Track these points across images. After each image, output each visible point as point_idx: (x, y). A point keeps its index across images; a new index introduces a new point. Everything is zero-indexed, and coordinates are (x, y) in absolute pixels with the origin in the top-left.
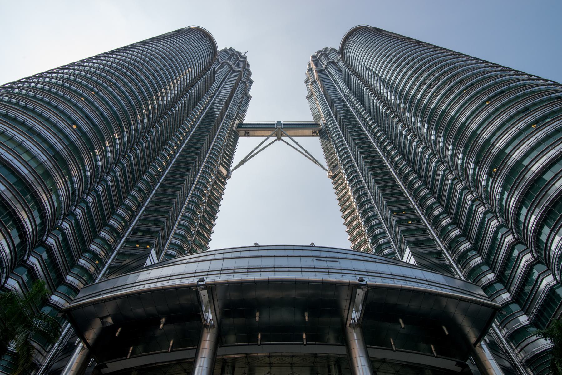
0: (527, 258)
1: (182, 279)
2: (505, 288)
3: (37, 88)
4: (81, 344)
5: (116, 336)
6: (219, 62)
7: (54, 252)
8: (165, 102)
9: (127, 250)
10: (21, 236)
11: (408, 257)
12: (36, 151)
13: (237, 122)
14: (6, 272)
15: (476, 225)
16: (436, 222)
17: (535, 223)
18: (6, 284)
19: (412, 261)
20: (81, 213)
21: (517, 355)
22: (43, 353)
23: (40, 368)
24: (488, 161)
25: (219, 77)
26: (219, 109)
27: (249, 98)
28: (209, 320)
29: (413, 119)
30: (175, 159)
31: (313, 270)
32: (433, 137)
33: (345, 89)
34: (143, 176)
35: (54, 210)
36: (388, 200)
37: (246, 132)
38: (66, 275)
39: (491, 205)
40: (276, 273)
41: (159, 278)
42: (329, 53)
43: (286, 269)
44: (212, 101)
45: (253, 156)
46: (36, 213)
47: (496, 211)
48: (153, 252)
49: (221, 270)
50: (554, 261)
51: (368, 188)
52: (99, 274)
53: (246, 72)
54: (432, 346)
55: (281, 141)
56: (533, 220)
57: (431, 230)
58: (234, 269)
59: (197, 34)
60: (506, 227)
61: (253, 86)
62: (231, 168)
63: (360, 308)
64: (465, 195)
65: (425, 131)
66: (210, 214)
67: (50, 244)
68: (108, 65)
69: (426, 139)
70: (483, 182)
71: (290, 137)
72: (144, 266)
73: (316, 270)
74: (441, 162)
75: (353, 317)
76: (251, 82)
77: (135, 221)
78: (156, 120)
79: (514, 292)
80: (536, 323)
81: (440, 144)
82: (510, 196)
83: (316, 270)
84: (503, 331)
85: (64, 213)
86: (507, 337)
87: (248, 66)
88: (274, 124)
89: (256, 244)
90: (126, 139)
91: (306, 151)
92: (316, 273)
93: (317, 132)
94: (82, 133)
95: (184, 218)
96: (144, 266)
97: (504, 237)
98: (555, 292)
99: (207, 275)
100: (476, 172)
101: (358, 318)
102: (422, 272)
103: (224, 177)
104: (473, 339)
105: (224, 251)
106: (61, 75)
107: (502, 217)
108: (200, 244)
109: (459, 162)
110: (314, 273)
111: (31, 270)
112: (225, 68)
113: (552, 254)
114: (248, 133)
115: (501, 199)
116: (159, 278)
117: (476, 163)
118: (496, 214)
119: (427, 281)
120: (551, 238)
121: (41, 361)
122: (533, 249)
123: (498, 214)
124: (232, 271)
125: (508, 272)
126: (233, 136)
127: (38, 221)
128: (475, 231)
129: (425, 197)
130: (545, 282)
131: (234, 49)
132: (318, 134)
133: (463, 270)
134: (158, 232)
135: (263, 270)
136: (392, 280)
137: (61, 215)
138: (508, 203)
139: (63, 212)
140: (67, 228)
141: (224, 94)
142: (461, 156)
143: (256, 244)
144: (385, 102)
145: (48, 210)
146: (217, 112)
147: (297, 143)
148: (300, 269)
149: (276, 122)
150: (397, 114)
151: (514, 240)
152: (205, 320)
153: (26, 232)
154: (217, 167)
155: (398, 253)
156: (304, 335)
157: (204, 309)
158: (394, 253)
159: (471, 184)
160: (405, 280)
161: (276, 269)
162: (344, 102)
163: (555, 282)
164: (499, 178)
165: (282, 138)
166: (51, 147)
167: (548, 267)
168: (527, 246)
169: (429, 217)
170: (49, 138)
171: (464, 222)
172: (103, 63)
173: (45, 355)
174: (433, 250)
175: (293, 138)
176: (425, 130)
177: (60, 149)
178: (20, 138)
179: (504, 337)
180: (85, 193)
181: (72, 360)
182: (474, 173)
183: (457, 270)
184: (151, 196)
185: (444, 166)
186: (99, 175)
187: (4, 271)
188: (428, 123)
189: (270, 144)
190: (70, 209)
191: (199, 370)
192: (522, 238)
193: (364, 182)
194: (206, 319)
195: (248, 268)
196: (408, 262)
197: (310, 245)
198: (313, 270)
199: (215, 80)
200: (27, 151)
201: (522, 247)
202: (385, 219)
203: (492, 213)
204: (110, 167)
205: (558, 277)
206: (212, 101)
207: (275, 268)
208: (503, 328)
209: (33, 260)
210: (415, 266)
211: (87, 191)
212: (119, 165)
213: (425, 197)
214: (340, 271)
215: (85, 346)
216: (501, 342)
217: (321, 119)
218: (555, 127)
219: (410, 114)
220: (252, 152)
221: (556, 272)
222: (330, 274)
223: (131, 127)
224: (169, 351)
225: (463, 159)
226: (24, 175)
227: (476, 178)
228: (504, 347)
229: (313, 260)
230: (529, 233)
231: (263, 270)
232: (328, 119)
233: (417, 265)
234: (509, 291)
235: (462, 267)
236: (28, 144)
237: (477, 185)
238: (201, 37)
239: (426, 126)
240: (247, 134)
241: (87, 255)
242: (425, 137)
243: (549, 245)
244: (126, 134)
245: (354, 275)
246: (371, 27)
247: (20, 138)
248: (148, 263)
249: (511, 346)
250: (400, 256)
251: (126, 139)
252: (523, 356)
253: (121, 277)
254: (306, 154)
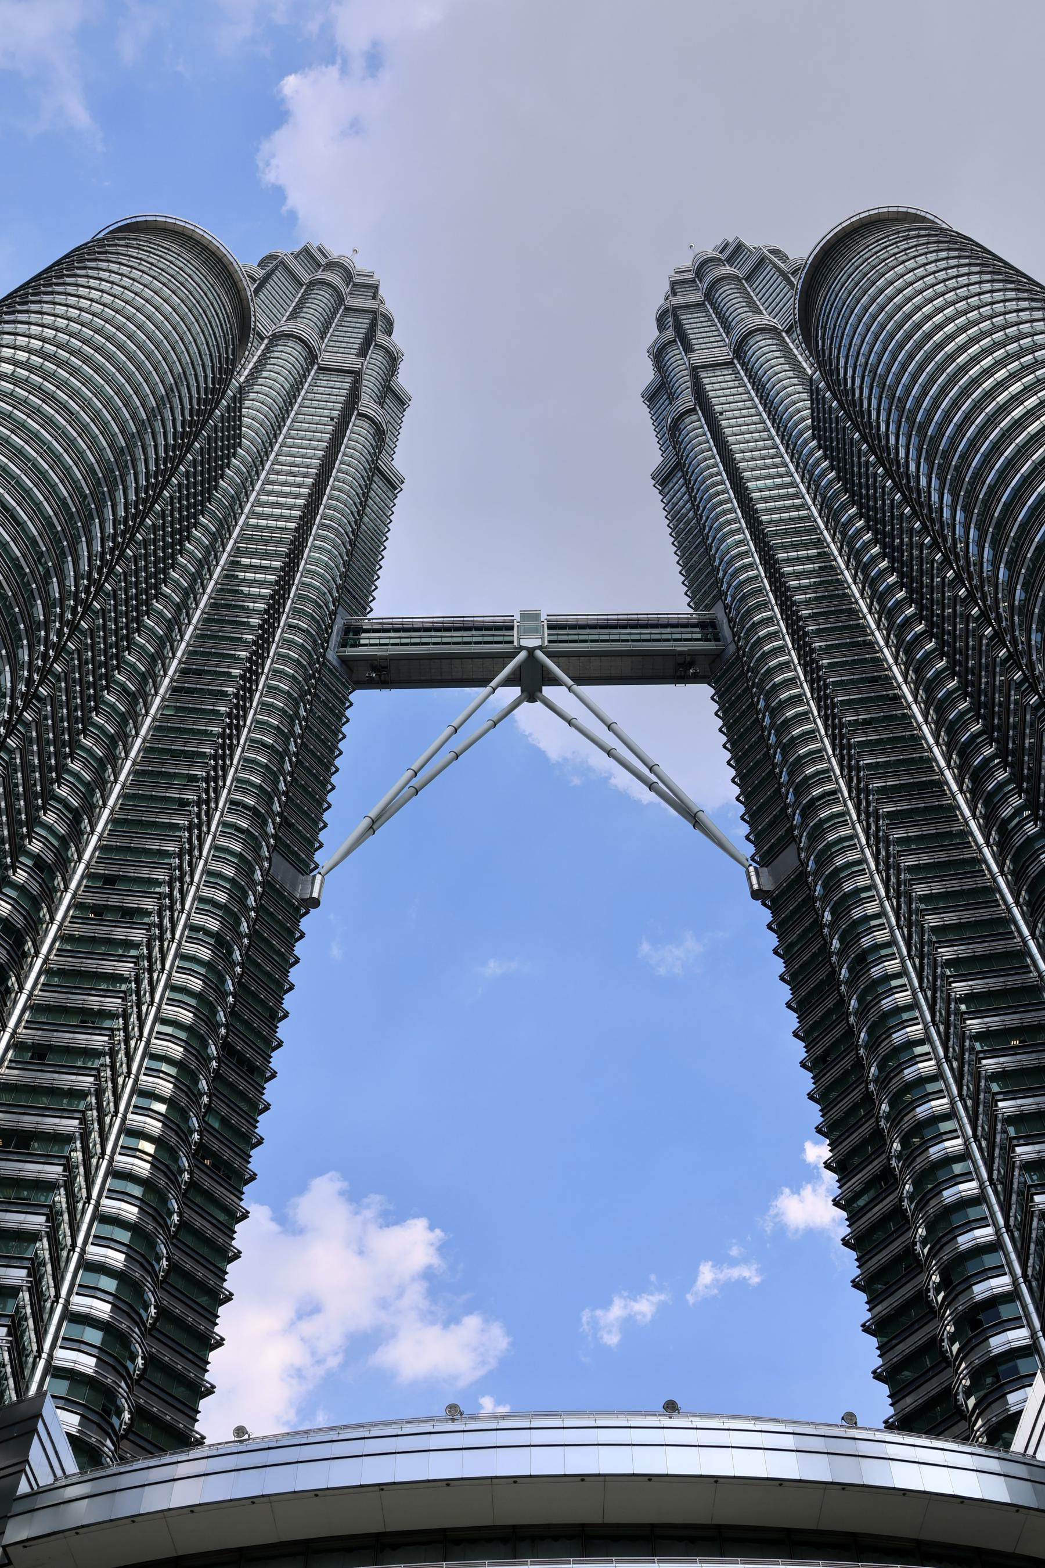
27: (393, 485)
55: (538, 704)
112: (289, 355)
149: (517, 618)
254: (654, 778)
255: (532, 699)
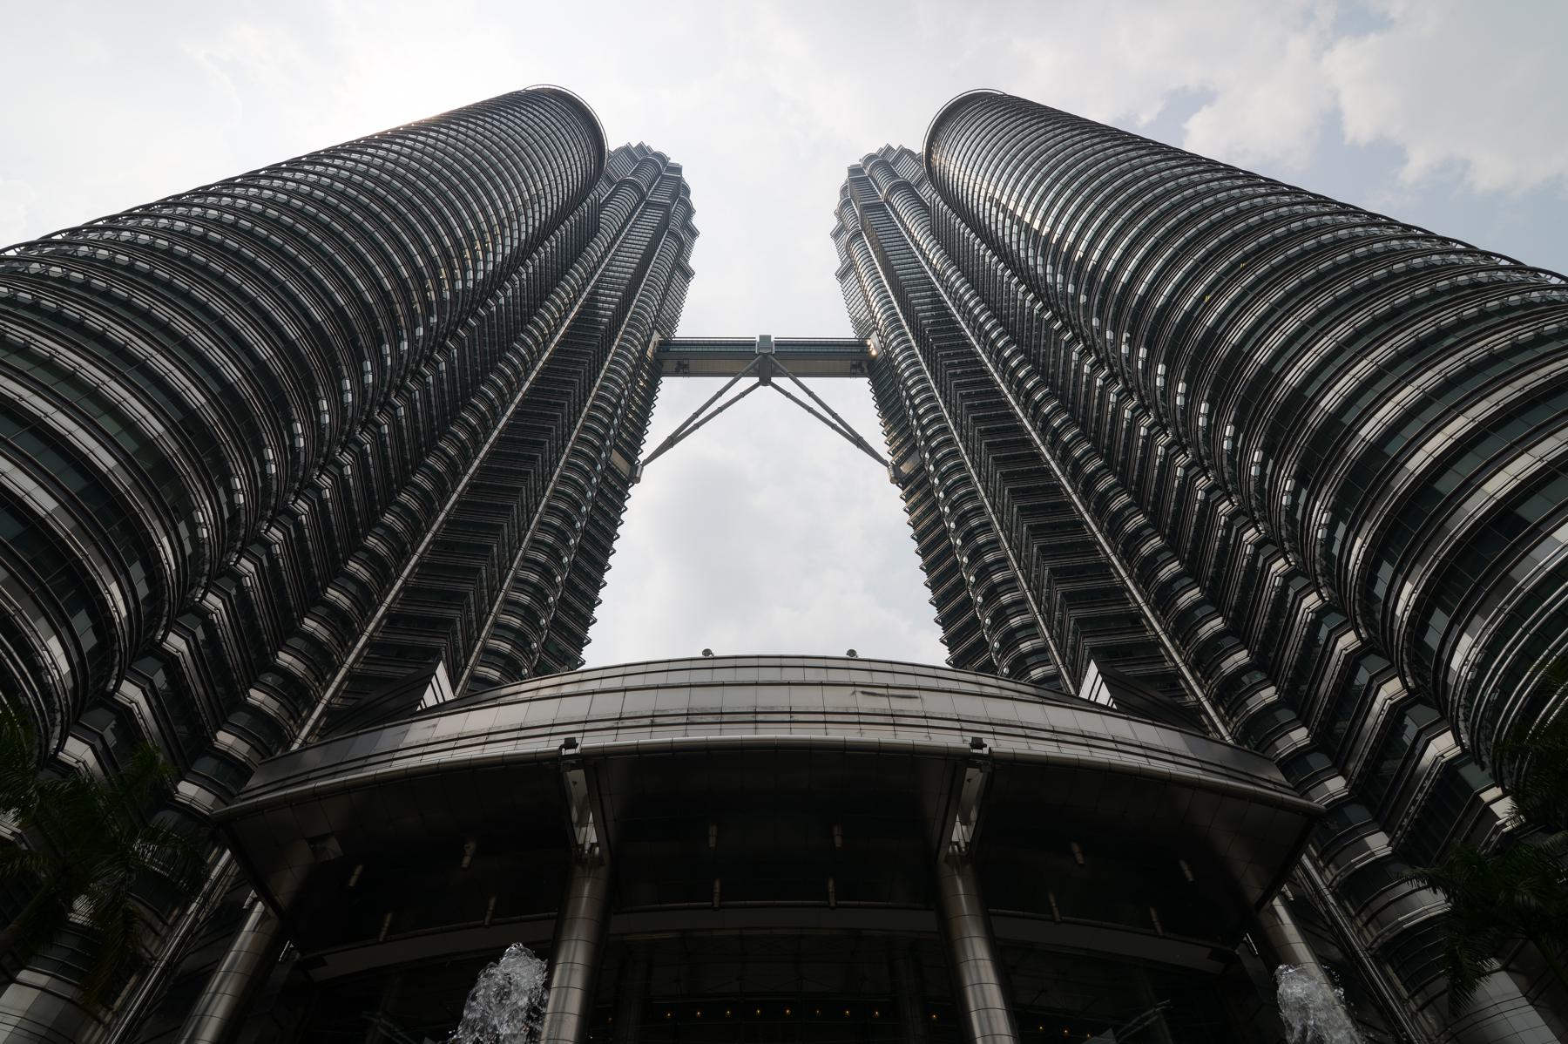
0: (1392, 689)
1: (520, 742)
2: (1335, 765)
3: (137, 244)
4: (259, 906)
5: (351, 884)
6: (611, 182)
7: (185, 670)
8: (470, 284)
9: (373, 668)
10: (97, 630)
11: (1093, 684)
12: (135, 408)
13: (656, 337)
14: (62, 721)
15: (1265, 607)
16: (1163, 598)
17: (1412, 603)
18: (60, 754)
19: (1104, 697)
20: (253, 570)
21: (1360, 932)
22: (158, 928)
23: (151, 967)
24: (1337, 475)
25: (610, 220)
26: (609, 303)
27: (688, 274)
28: (587, 846)
29: (1109, 335)
30: (496, 433)
31: (855, 718)
32: (1159, 382)
33: (935, 257)
34: (414, 475)
35: (183, 561)
36: (1043, 541)
37: (679, 364)
38: (217, 731)
39: (1303, 556)
40: (760, 725)
41: (458, 739)
42: (895, 162)
43: (786, 717)
44: (593, 281)
45: (697, 426)
46: (136, 571)
47: (1315, 571)
48: (441, 671)
49: (620, 719)
50: (1457, 698)
51: (993, 512)
52: (301, 728)
53: (682, 208)
54: (1153, 912)
55: (770, 387)
56: (1408, 594)
57: (1152, 620)
58: (654, 716)
59: (554, 107)
60: (1342, 612)
61: (698, 242)
62: (642, 458)
63: (973, 815)
64: (1238, 530)
65: (1140, 366)
66: (588, 575)
67: (173, 650)
68: (322, 186)
69: (1142, 387)
70: (1285, 498)
71: (794, 376)
72: (419, 709)
73: (863, 719)
74: (1178, 445)
75: (955, 838)
76: (694, 234)
77: (393, 593)
78: (447, 330)
79: (1355, 775)
80: (1407, 854)
81: (1178, 398)
82: (1352, 534)
83: (863, 719)
84: (1327, 872)
85: (210, 571)
86: (1337, 886)
87: (687, 191)
88: (752, 344)
89: (707, 652)
90: (369, 379)
91: (834, 415)
92: (863, 727)
93: (864, 365)
94: (254, 363)
95: (521, 586)
96: (419, 709)
97: (1333, 637)
98: (1458, 775)
99: (584, 731)
100: (1269, 471)
101: (968, 840)
102: (1131, 727)
103: (624, 480)
104: (1254, 893)
105: (626, 670)
106: (199, 210)
107: (1332, 586)
108: (560, 651)
109: (1225, 447)
110: (858, 726)
111: (125, 715)
112: (628, 197)
113: (1451, 680)
114: (686, 366)
115: (1330, 540)
116: (458, 739)
117: (1268, 450)
118: (1317, 579)
119: (1141, 747)
120: (1452, 639)
121: (153, 949)
122: (1405, 667)
123: (1320, 580)
124: (647, 721)
125: (1342, 726)
126: (647, 373)
127: (143, 591)
128: (1262, 621)
129: (1138, 536)
130: (1433, 750)
131: (649, 148)
132: (866, 371)
133: (1231, 719)
134: (452, 622)
135: (726, 718)
136: (1055, 744)
137: (202, 575)
138: (1347, 549)
139: (207, 567)
140: (216, 608)
141: (625, 267)
142: (1229, 431)
143: (707, 652)
144: (1040, 290)
145: (168, 563)
146: (605, 309)
147: (811, 394)
148: (821, 718)
149: (758, 340)
150: (1070, 322)
151: (1359, 644)
152: (578, 846)
153: (113, 619)
154: (604, 455)
155: (1066, 677)
156: (831, 884)
157: (575, 816)
158: (1056, 677)
159: (1253, 502)
160: (1087, 745)
161: (760, 717)
162: (934, 289)
163: (1458, 750)
164: (1325, 489)
165: (774, 380)
166: (175, 398)
167: (1441, 713)
168: (1392, 661)
169: (1146, 586)
170: (171, 375)
171: (1234, 598)
172: (309, 179)
173: (164, 932)
174: (1157, 669)
175: (801, 379)
176: (1140, 363)
177: (199, 405)
178: (92, 373)
179: (1328, 887)
180: (262, 518)
181: (236, 947)
182: (1262, 475)
183: (1216, 720)
184: (435, 527)
185: (1187, 456)
186: (301, 474)
187: (55, 719)
188: (1148, 346)
189: (743, 395)
190: (224, 560)
191: (563, 970)
192: (1377, 640)
193: (983, 494)
194: (580, 842)
195: (688, 714)
196: (1092, 699)
197: (844, 655)
198: (855, 718)
199: (599, 227)
200: (113, 410)
201: (1376, 663)
202: (1036, 590)
203: (1305, 575)
204: (328, 452)
205: (1465, 739)
206: (593, 281)
207: (756, 713)
208: (1327, 866)
209: (130, 692)
210: (1111, 709)
211: (269, 513)
212: (352, 446)
213: (1138, 536)
214: (923, 722)
215: (270, 911)
216: (1323, 899)
217: (875, 333)
218: (1466, 358)
219: (1101, 323)
220: (696, 415)
221: (1462, 725)
222: (897, 728)
223: (383, 347)
224: (486, 924)
225: (1235, 439)
226: (105, 470)
227: (1266, 486)
228: (1328, 912)
229: (854, 693)
230: (1396, 627)
231: (726, 718)
232: (892, 332)
233: (1114, 707)
234: (1343, 773)
235: (1227, 713)
236: (115, 390)
237: (1269, 504)
238: (564, 115)
239: (1142, 352)
240: (682, 370)
241: (269, 679)
242: (1141, 380)
243: (1445, 657)
244: (368, 365)
245: (958, 733)
246: (1005, 94)
247: (92, 373)
248: (429, 699)
249: (1345, 909)
250: (1072, 683)
251: (369, 379)
252: (1375, 935)
253: (361, 737)
254: (834, 421)
255: (765, 385)
